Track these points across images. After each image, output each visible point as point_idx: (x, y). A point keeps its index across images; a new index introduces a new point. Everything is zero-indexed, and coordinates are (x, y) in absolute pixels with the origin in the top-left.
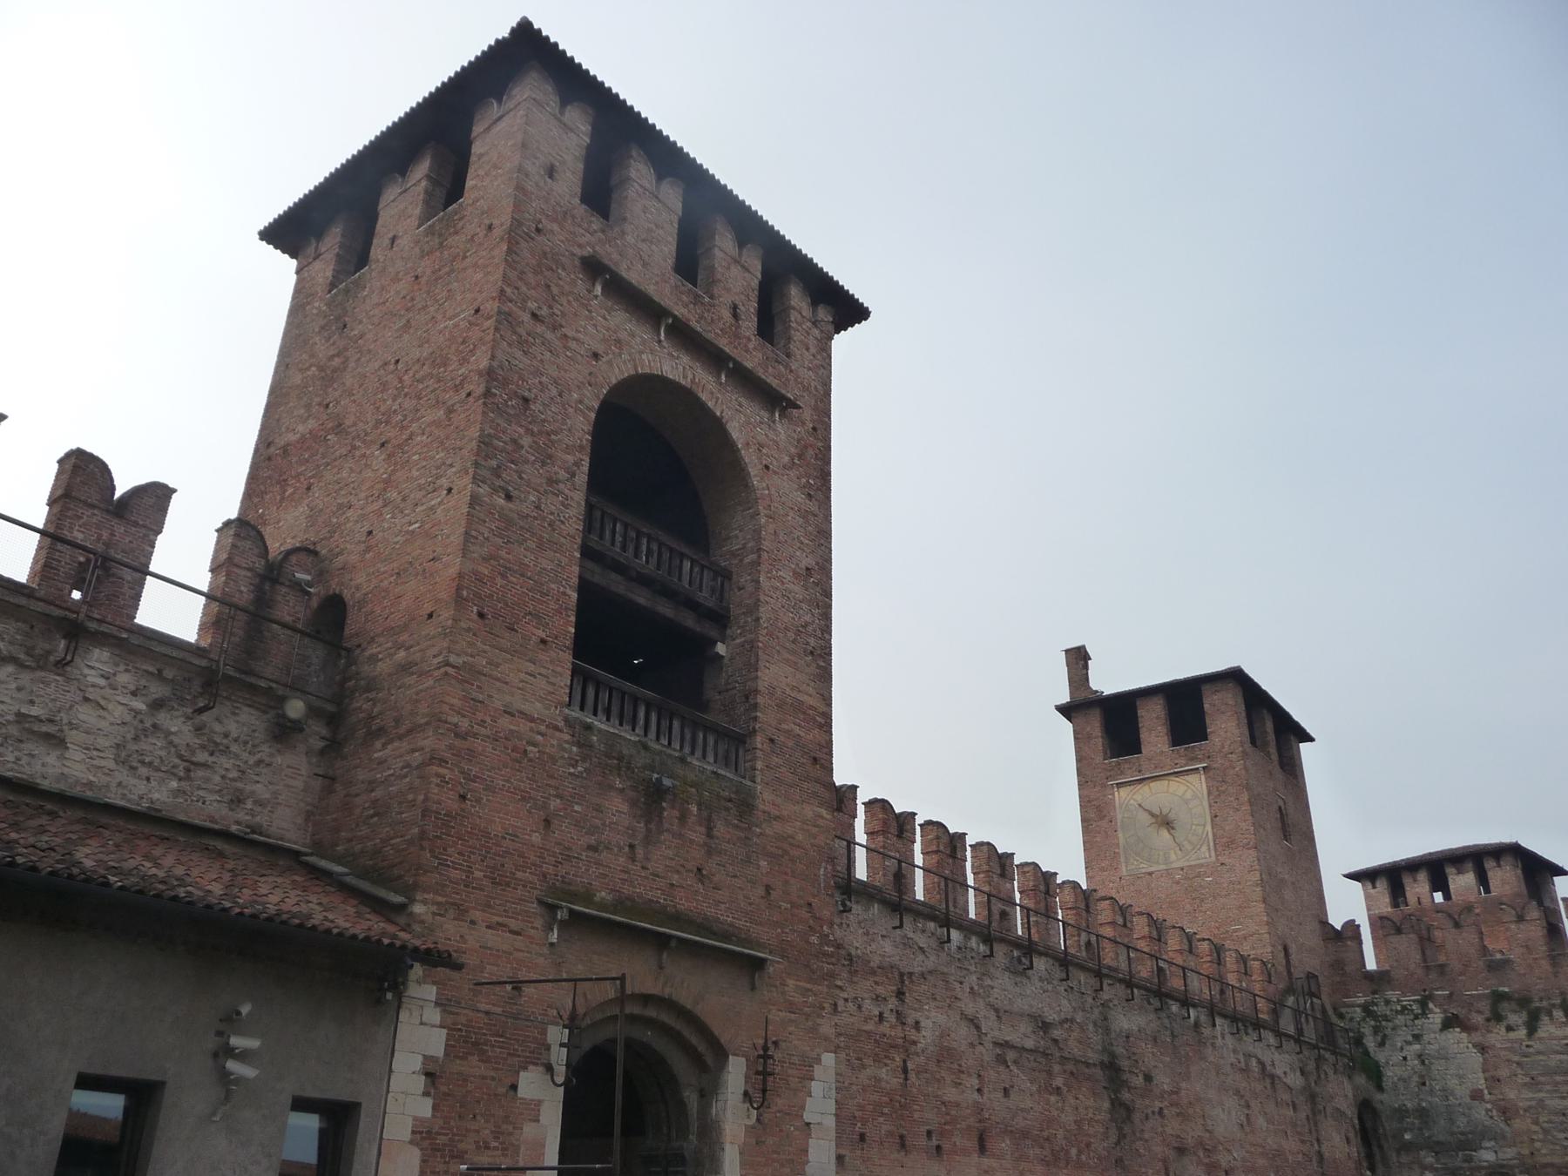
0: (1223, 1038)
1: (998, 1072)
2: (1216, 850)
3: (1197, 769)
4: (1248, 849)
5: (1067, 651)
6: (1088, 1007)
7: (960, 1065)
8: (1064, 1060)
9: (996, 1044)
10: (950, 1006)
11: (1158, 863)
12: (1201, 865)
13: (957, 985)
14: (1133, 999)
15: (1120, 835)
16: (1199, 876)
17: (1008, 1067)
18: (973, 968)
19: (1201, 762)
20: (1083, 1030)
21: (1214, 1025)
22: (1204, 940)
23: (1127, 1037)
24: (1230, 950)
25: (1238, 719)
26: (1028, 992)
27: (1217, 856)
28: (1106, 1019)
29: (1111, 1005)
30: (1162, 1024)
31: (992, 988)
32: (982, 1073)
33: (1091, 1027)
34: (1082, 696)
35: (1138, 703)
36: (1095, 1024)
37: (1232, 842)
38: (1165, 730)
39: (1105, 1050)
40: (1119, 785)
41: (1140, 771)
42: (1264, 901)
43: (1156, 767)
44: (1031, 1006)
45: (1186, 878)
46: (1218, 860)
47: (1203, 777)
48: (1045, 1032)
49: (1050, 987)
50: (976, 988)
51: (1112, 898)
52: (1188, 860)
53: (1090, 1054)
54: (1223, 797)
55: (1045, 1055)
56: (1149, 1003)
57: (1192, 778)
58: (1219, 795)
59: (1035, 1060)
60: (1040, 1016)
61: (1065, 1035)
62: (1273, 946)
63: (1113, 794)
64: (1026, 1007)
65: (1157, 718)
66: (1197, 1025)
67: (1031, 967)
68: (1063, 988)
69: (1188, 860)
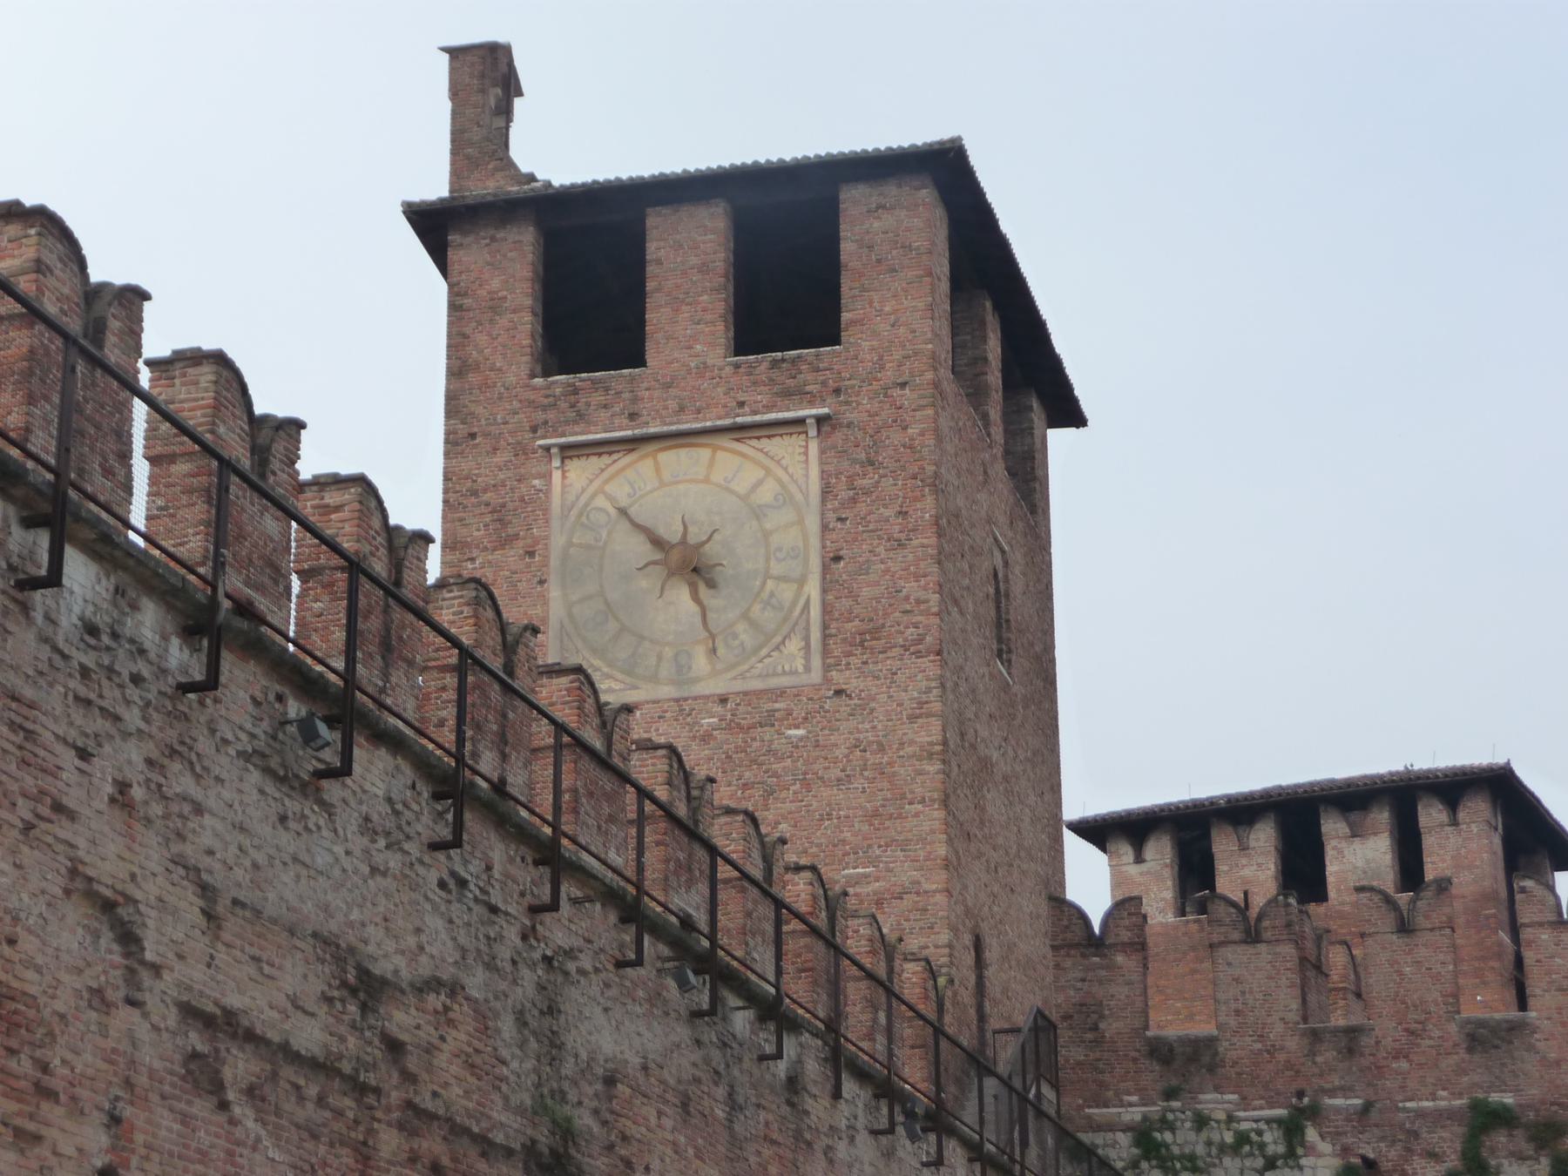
0: (852, 1139)
1: (185, 1119)
2: (826, 652)
3: (800, 421)
4: (918, 655)
5: (455, 53)
6: (504, 953)
7: (45, 1068)
8: (415, 1117)
9: (189, 1012)
10: (28, 827)
11: (654, 679)
12: (781, 693)
13: (68, 758)
14: (639, 962)
15: (554, 592)
16: (769, 720)
17: (224, 1106)
18: (133, 718)
19: (811, 404)
20: (485, 1029)
21: (837, 1095)
22: (798, 868)
23: (610, 1081)
24: (855, 916)
25: (933, 292)
26: (322, 860)
27: (827, 668)
28: (552, 1010)
29: (571, 966)
30: (707, 1061)
31: (199, 810)
32: (127, 1112)
33: (507, 1026)
34: (486, 187)
35: (651, 222)
36: (521, 1021)
37: (875, 633)
38: (720, 307)
39: (540, 1109)
40: (568, 451)
41: (633, 416)
42: (945, 803)
43: (682, 409)
44: (326, 908)
45: (732, 726)
46: (827, 680)
47: (814, 447)
48: (364, 1008)
49: (394, 861)
50: (137, 793)
51: (579, 670)
52: (742, 676)
53: (499, 1115)
54: (862, 508)
55: (360, 1089)
56: (684, 985)
57: (784, 447)
58: (854, 500)
59: (321, 1101)
60: (352, 950)
61: (428, 1033)
62: (954, 929)
63: (547, 476)
64: (308, 907)
65: (703, 269)
66: (793, 1083)
67: (345, 770)
68: (433, 877)
69: (742, 676)
